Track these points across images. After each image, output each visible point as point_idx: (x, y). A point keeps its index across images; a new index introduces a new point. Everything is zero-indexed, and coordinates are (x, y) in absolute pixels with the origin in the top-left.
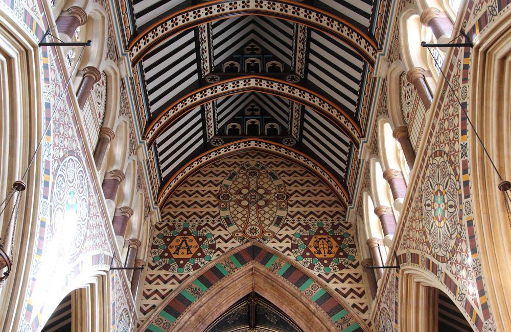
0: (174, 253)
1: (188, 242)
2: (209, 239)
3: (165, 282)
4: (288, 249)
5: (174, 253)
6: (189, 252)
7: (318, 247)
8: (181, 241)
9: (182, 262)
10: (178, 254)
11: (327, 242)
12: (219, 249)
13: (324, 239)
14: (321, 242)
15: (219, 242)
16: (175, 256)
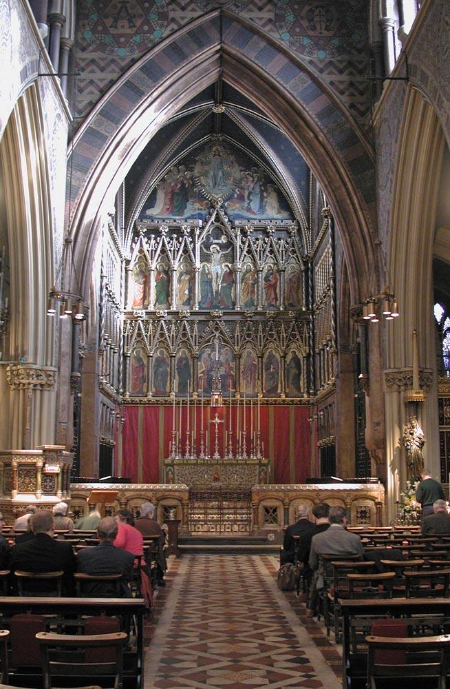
0: (111, 27)
1: (129, 8)
2: (159, 4)
3: (102, 69)
4: (270, 20)
5: (111, 27)
6: (132, 24)
7: (312, 20)
8: (119, 8)
9: (122, 40)
10: (116, 27)
11: (326, 12)
12: (173, 20)
13: (322, 7)
14: (317, 12)
15: (174, 10)
16: (112, 31)
